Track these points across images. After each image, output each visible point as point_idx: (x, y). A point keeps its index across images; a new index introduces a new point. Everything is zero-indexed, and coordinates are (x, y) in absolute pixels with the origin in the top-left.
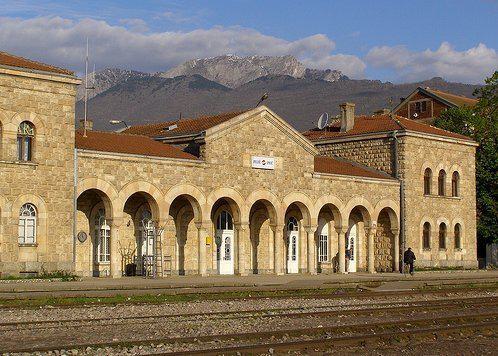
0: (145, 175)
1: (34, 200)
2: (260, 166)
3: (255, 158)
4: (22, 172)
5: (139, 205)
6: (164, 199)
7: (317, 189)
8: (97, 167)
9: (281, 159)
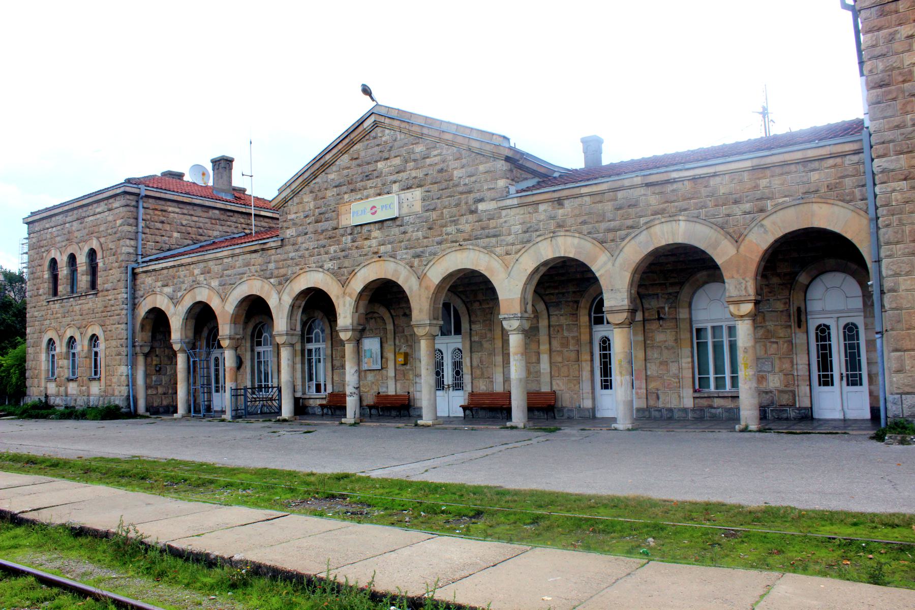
0: (201, 278)
1: (98, 331)
4: (91, 303)
6: (225, 309)
7: (518, 228)
9: (418, 193)
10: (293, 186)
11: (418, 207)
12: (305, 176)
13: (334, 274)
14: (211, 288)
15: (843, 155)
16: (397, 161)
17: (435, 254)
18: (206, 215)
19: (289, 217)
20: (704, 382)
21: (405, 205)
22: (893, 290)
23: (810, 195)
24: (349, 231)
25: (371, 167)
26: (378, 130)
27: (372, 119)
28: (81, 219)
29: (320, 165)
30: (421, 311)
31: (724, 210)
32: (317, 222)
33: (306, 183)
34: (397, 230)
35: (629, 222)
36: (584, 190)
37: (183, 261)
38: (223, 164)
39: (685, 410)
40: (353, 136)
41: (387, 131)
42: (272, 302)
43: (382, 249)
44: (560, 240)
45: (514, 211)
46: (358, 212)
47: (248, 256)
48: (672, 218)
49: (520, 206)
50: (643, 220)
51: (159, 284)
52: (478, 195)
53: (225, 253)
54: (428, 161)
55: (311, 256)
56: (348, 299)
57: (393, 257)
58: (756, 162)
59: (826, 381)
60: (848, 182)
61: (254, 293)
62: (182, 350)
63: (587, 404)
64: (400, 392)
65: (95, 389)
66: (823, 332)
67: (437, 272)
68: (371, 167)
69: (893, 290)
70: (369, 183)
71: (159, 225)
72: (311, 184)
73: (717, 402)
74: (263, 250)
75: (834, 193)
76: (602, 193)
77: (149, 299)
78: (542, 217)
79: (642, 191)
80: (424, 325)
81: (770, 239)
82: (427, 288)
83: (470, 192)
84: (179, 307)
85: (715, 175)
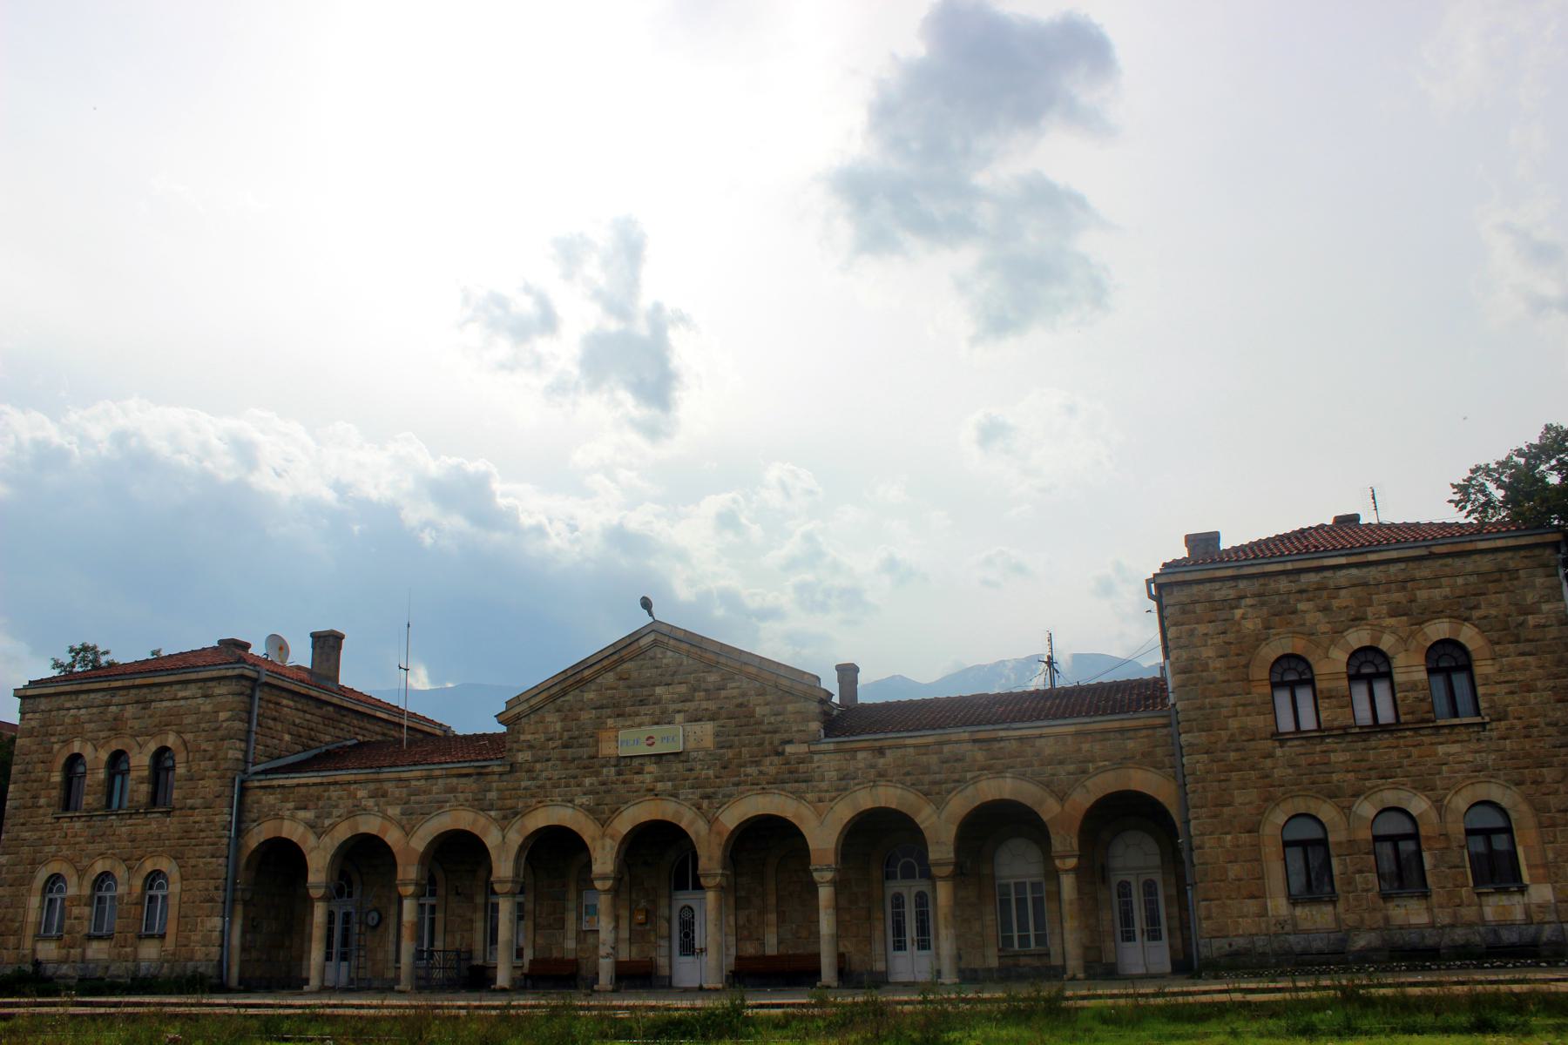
0: (371, 802)
1: (165, 865)
2: (644, 750)
3: (622, 734)
4: (153, 824)
5: (364, 858)
6: (410, 845)
8: (285, 800)
9: (709, 727)
10: (533, 702)
11: (709, 742)
12: (553, 691)
13: (590, 811)
14: (385, 817)
15: (1154, 727)
16: (683, 689)
17: (730, 796)
18: (318, 712)
19: (522, 737)
20: (1008, 941)
21: (691, 739)
22: (1200, 847)
23: (1124, 761)
24: (613, 762)
25: (645, 692)
26: (658, 652)
27: (652, 637)
28: (145, 703)
29: (575, 679)
30: (710, 859)
31: (1049, 769)
32: (566, 746)
33: (552, 699)
34: (680, 766)
35: (956, 776)
36: (908, 741)
37: (338, 778)
38: (328, 644)
39: (990, 970)
40: (623, 653)
41: (669, 654)
42: (492, 839)
43: (659, 786)
44: (881, 790)
45: (826, 757)
46: (631, 741)
47: (455, 781)
48: (999, 773)
49: (836, 751)
50: (969, 775)
51: (291, 805)
52: (786, 736)
53: (418, 774)
54: (723, 693)
55: (555, 787)
56: (608, 842)
57: (675, 796)
58: (1079, 727)
59: (1128, 936)
60: (1159, 751)
61: (462, 827)
62: (325, 898)
63: (880, 966)
64: (635, 955)
65: (149, 952)
66: (1124, 890)
67: (733, 816)
68: (645, 692)
69: (1200, 847)
70: (643, 710)
71: (271, 723)
72: (559, 702)
73: (1023, 961)
74: (479, 774)
75: (1147, 760)
76: (927, 746)
77: (265, 826)
78: (861, 765)
79: (969, 746)
80: (715, 876)
81: (1093, 799)
82: (719, 833)
83: (775, 732)
84: (326, 840)
85: (1041, 736)
